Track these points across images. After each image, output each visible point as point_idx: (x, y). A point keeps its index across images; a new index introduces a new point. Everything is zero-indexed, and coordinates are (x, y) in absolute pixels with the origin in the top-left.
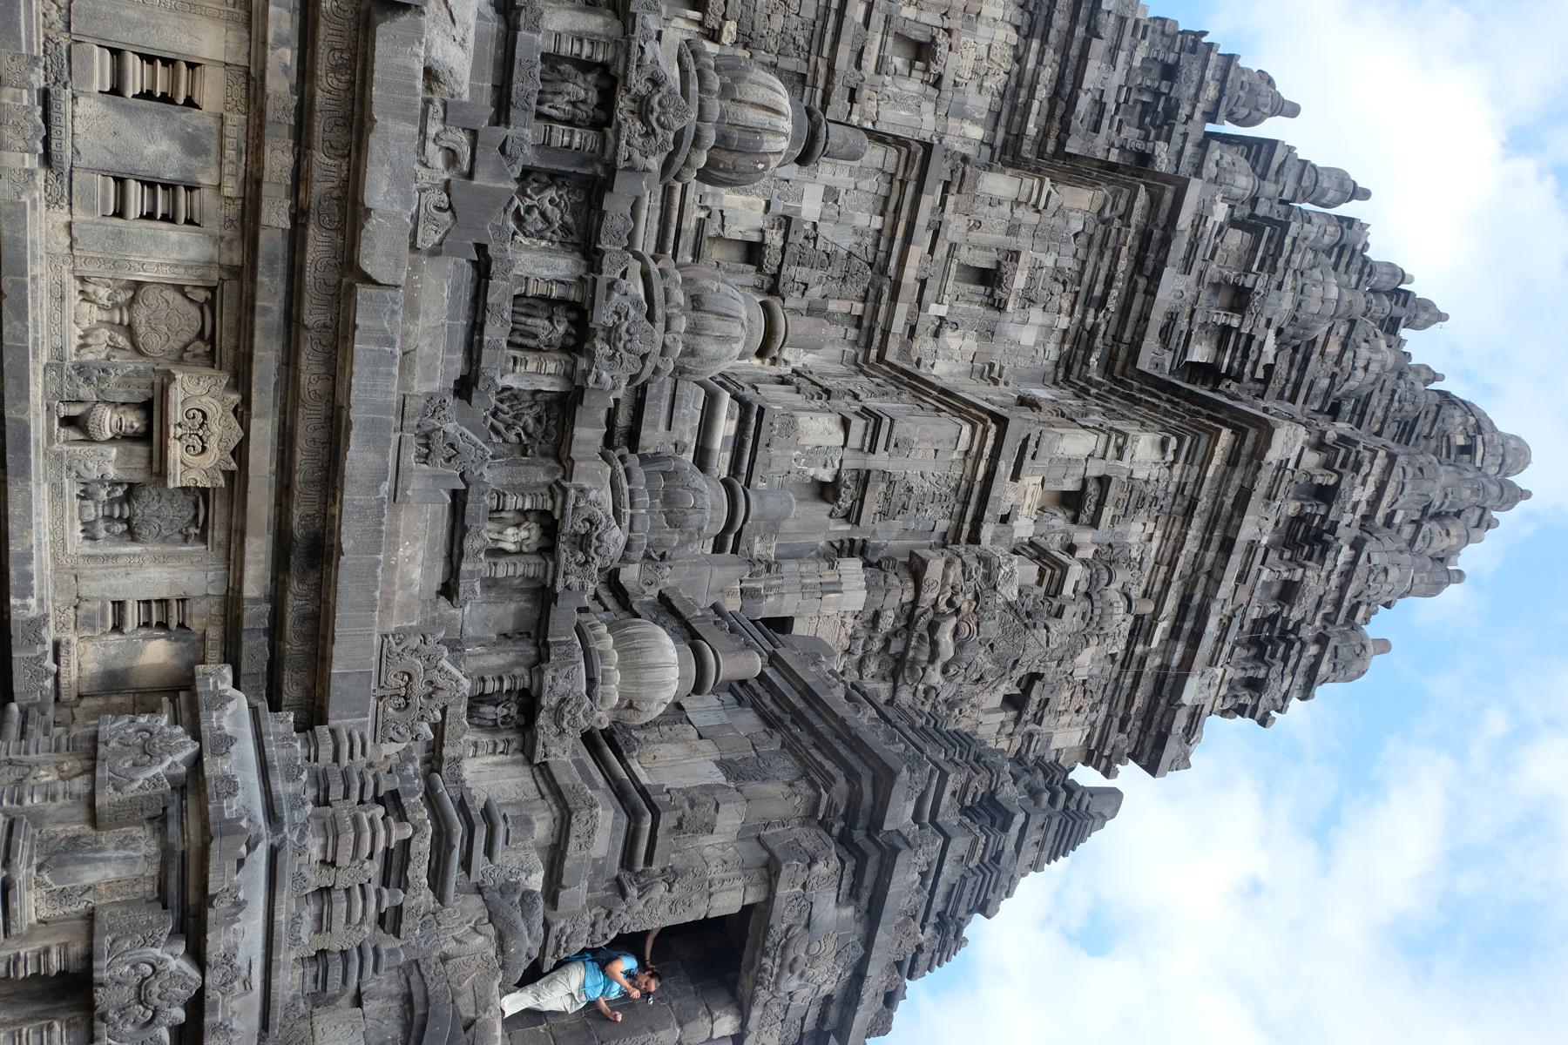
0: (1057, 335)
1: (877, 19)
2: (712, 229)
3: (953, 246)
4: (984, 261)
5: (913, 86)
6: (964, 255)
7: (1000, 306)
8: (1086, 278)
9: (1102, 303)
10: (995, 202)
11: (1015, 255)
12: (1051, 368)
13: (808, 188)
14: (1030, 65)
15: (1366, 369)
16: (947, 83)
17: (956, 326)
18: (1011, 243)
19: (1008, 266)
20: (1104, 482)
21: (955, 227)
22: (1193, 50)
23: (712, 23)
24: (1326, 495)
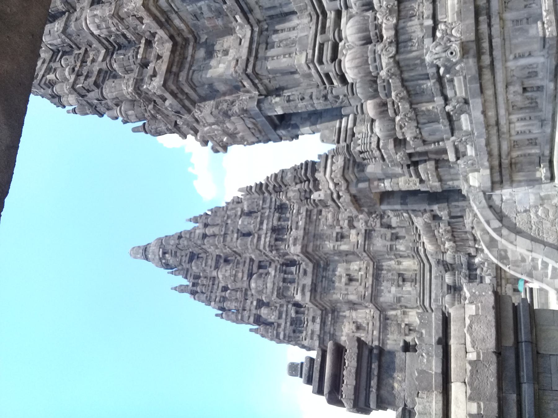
0: (331, 269)
1: (370, 332)
2: (413, 284)
3: (361, 284)
4: (354, 283)
5: (359, 321)
6: (358, 284)
7: (347, 275)
8: (327, 282)
9: (323, 277)
10: (352, 294)
11: (346, 284)
12: (331, 263)
13: (394, 292)
14: (332, 329)
15: (226, 270)
16: (351, 323)
17: (356, 270)
18: (347, 287)
19: (347, 282)
20: (337, 241)
21: (361, 289)
22: (289, 337)
23: (407, 327)
24: (276, 240)
